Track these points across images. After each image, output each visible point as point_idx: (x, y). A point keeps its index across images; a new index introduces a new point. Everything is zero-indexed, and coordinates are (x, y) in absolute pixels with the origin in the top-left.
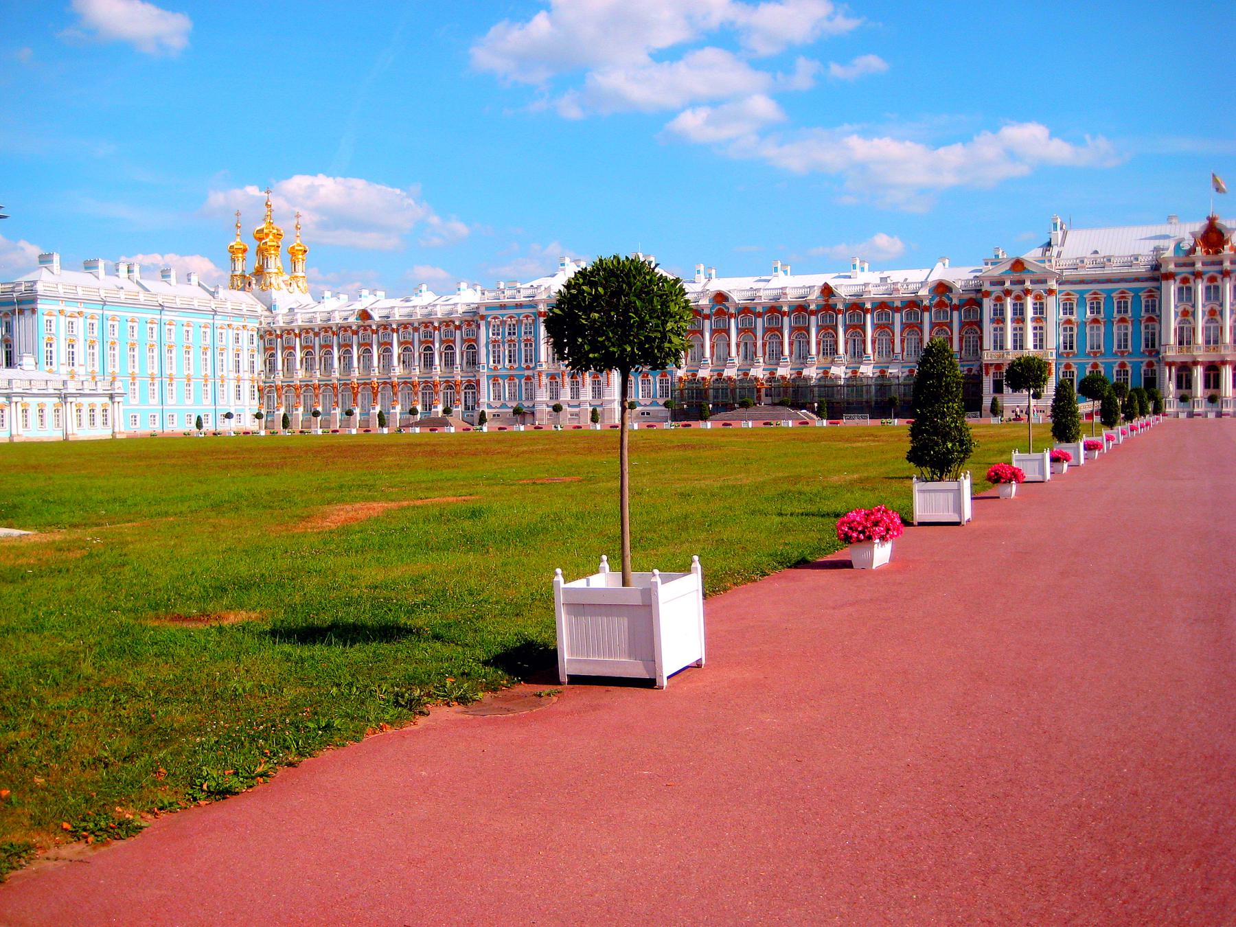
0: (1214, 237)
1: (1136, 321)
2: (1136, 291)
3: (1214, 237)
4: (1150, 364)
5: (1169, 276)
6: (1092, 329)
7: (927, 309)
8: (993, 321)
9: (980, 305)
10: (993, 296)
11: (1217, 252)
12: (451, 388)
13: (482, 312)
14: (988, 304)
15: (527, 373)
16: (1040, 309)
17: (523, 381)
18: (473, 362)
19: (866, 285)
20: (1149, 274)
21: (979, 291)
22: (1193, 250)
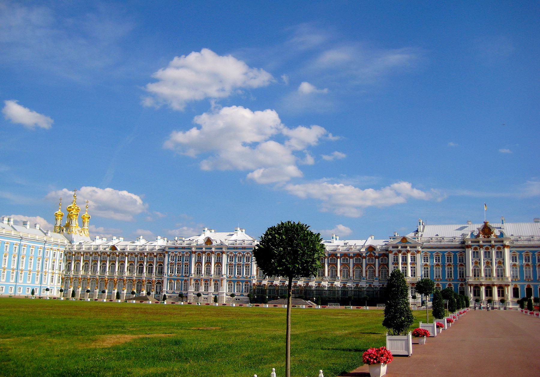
0: (487, 230)
1: (455, 266)
2: (455, 253)
3: (487, 230)
4: (462, 285)
5: (469, 247)
6: (436, 268)
7: (365, 257)
8: (393, 264)
9: (388, 256)
10: (393, 253)
11: (488, 237)
12: (150, 283)
13: (167, 250)
14: (391, 256)
15: (185, 278)
16: (414, 259)
17: (183, 282)
18: (161, 271)
19: (338, 246)
20: (460, 246)
21: (387, 250)
22: (478, 236)
